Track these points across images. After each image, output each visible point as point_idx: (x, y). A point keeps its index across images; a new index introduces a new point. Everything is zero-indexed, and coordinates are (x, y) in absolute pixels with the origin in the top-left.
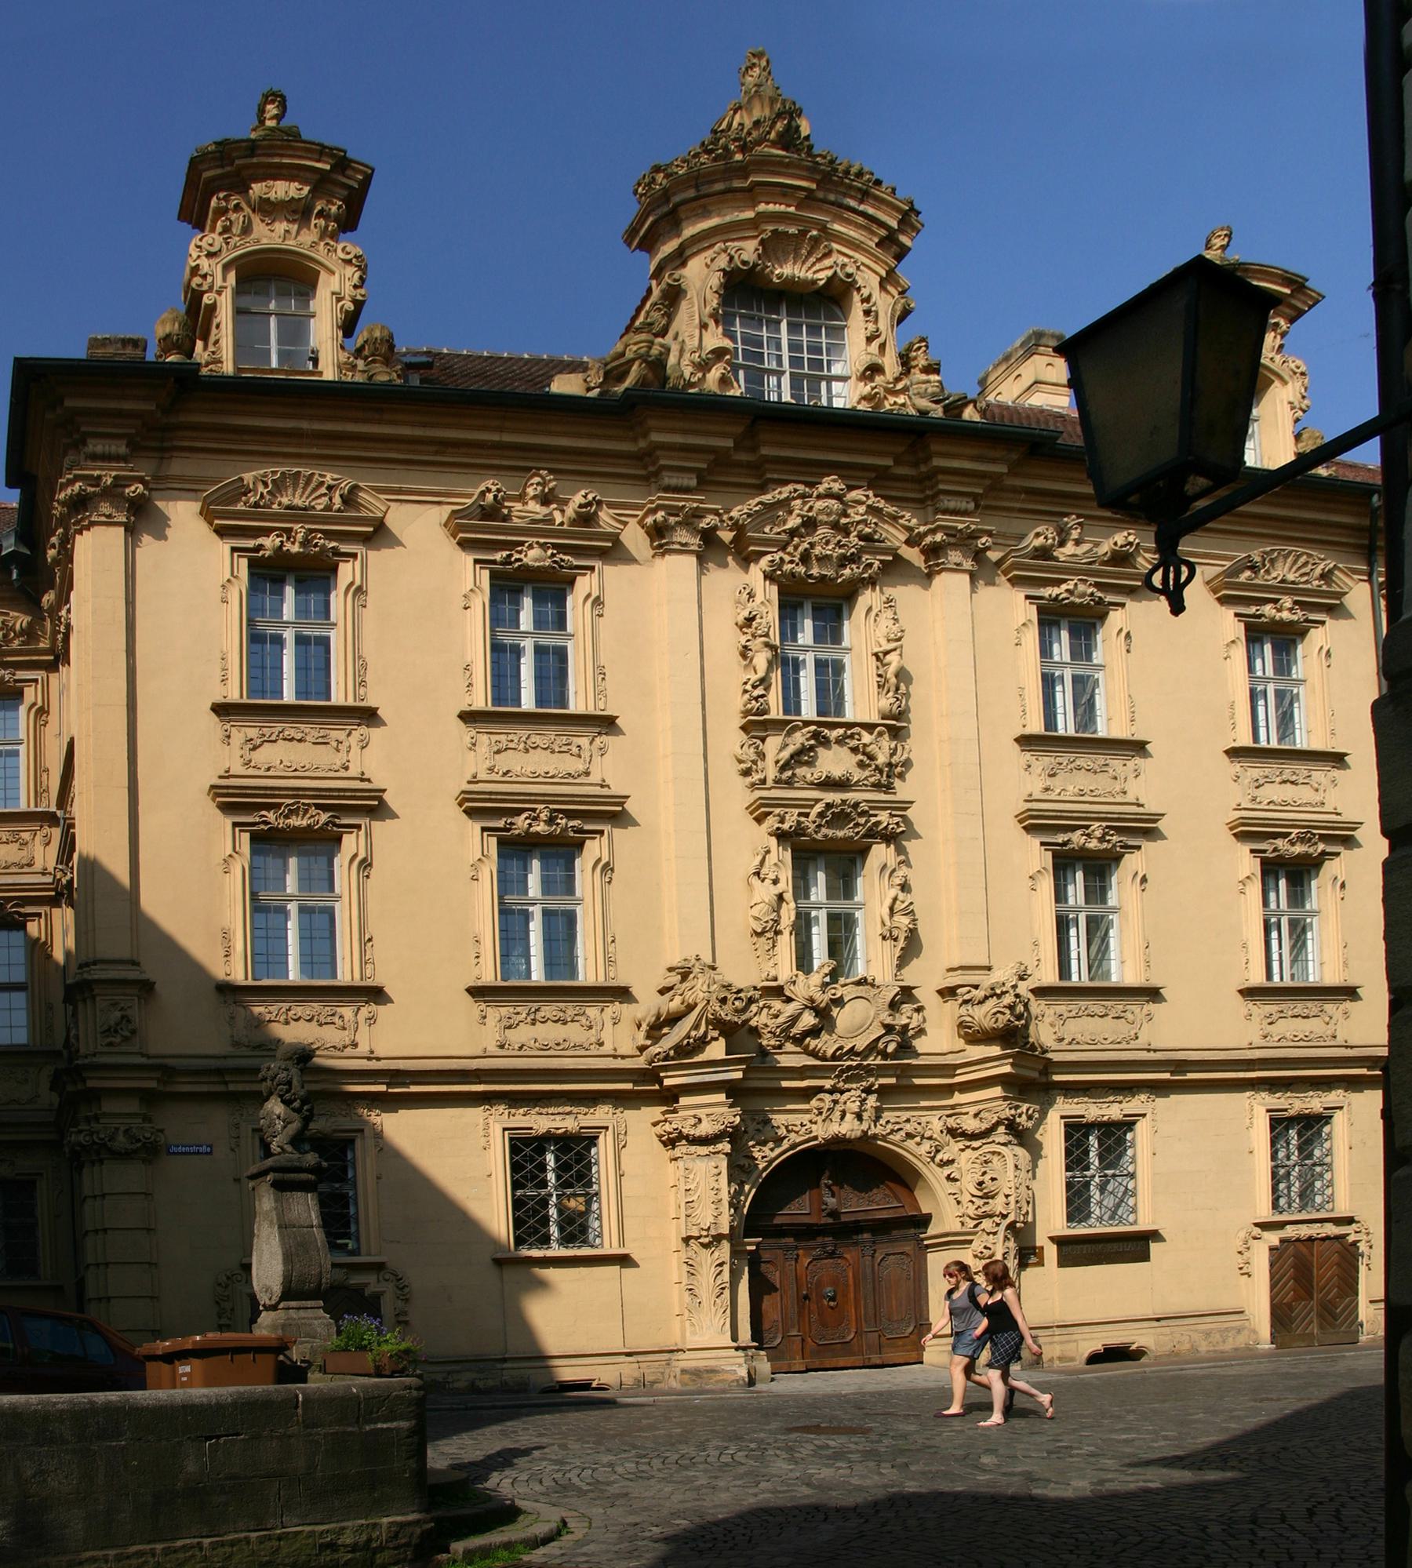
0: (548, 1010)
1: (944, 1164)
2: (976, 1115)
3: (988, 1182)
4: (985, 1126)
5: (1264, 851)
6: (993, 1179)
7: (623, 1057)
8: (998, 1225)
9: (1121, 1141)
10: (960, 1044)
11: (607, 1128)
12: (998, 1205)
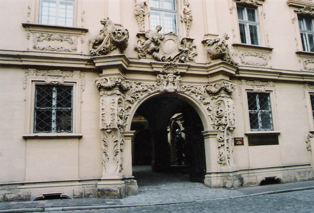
0: (56, 36)
1: (206, 104)
2: (215, 86)
3: (220, 112)
4: (217, 90)
5: (298, 12)
6: (221, 111)
7: (85, 55)
8: (224, 128)
9: (266, 100)
10: (210, 60)
11: (76, 83)
12: (223, 121)
